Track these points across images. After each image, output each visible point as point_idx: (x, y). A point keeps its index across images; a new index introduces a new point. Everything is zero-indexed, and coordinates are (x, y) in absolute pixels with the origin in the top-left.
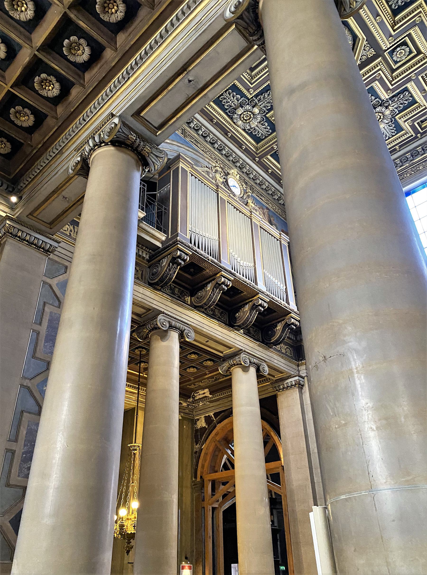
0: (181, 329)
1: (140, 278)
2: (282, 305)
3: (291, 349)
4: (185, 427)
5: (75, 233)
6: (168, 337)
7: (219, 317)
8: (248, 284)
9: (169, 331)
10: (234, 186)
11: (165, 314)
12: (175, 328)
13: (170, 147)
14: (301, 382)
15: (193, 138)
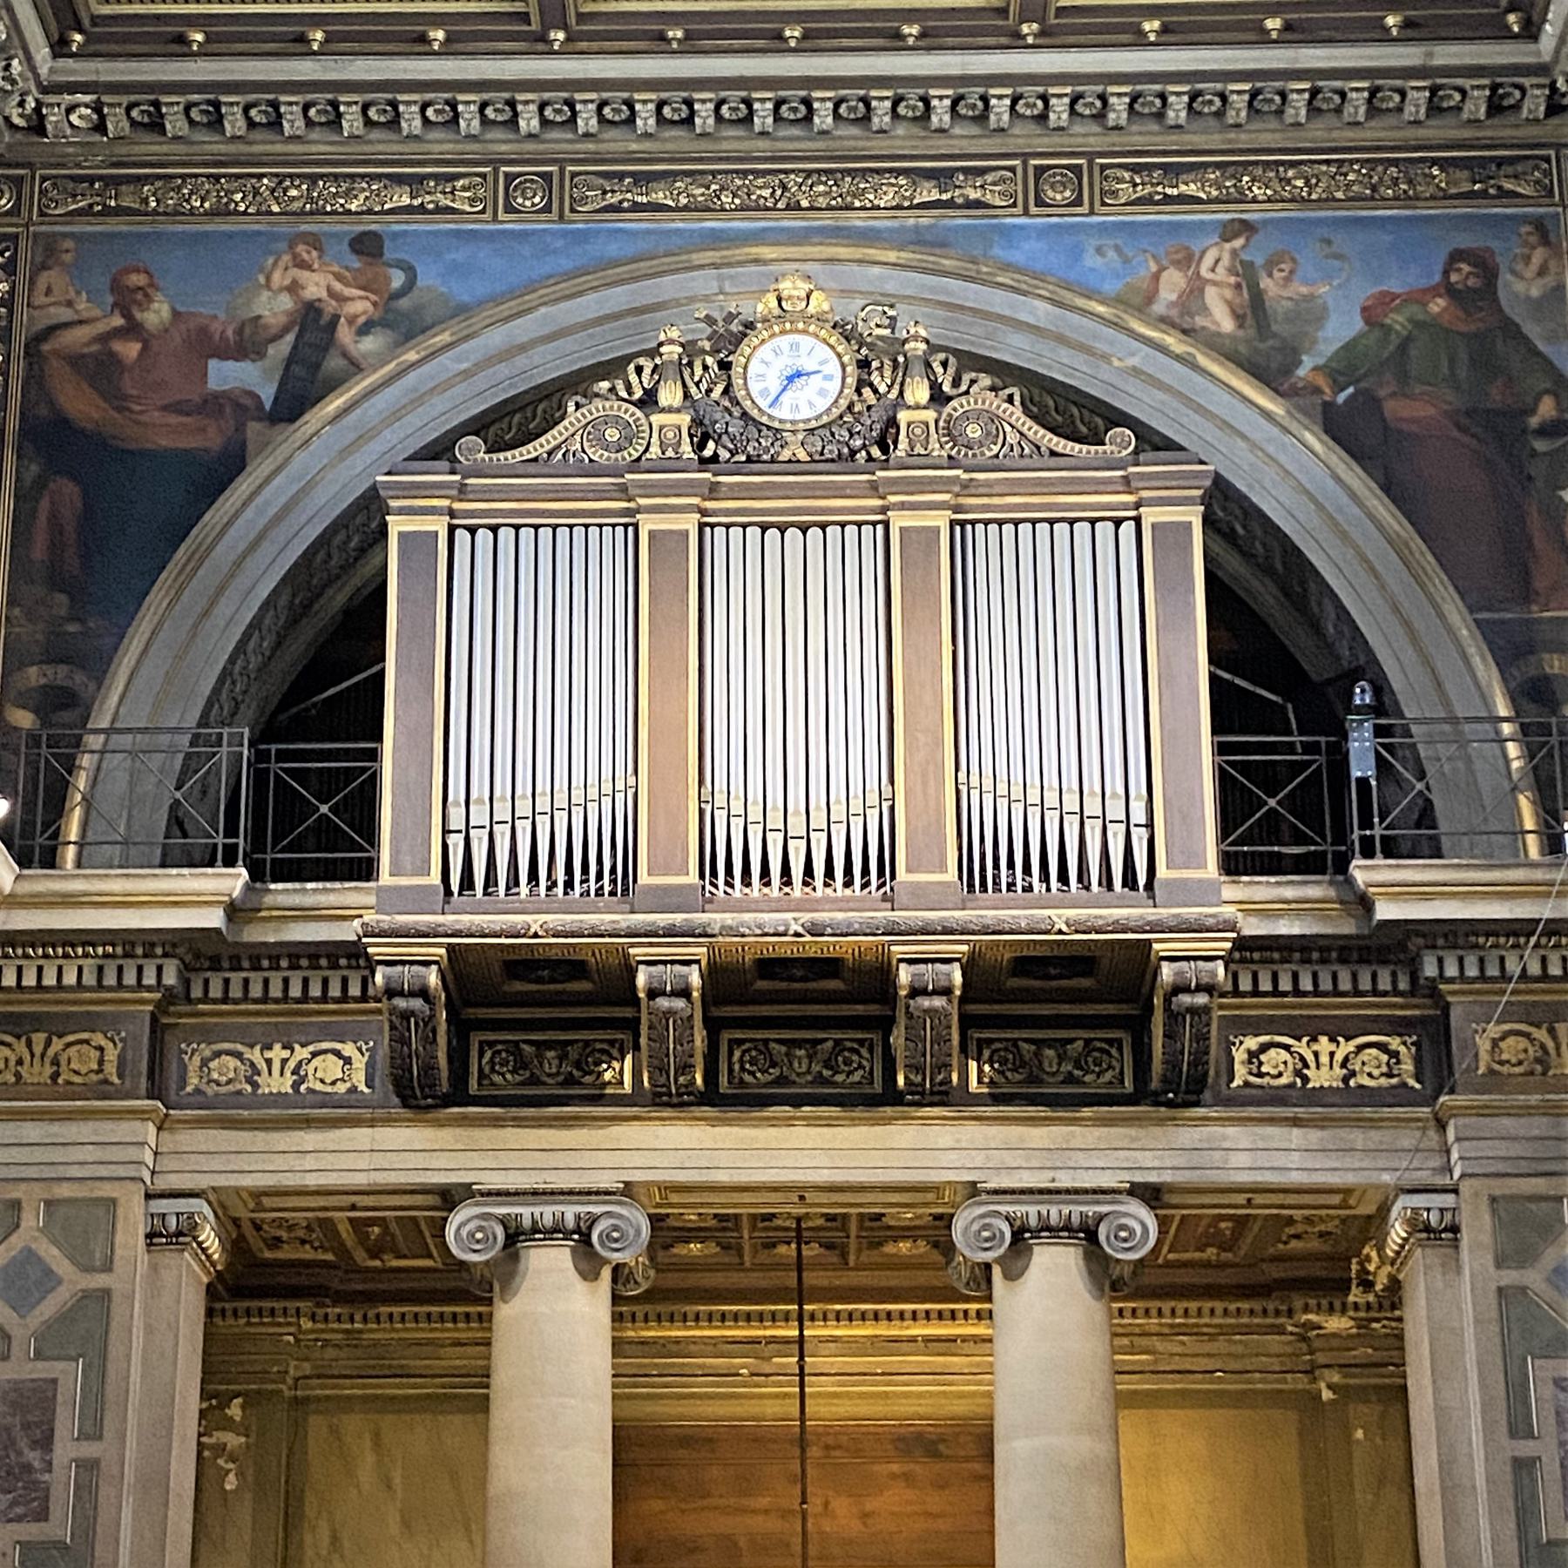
0: (570, 1223)
1: (363, 1088)
2: (1060, 932)
3: (1395, 1043)
4: (1359, 1434)
5: (37, 1060)
6: (518, 1279)
7: (820, 1080)
8: (797, 935)
9: (522, 1252)
10: (790, 379)
11: (482, 1195)
12: (540, 1232)
13: (459, 360)
14: (1434, 1219)
15: (621, 176)
